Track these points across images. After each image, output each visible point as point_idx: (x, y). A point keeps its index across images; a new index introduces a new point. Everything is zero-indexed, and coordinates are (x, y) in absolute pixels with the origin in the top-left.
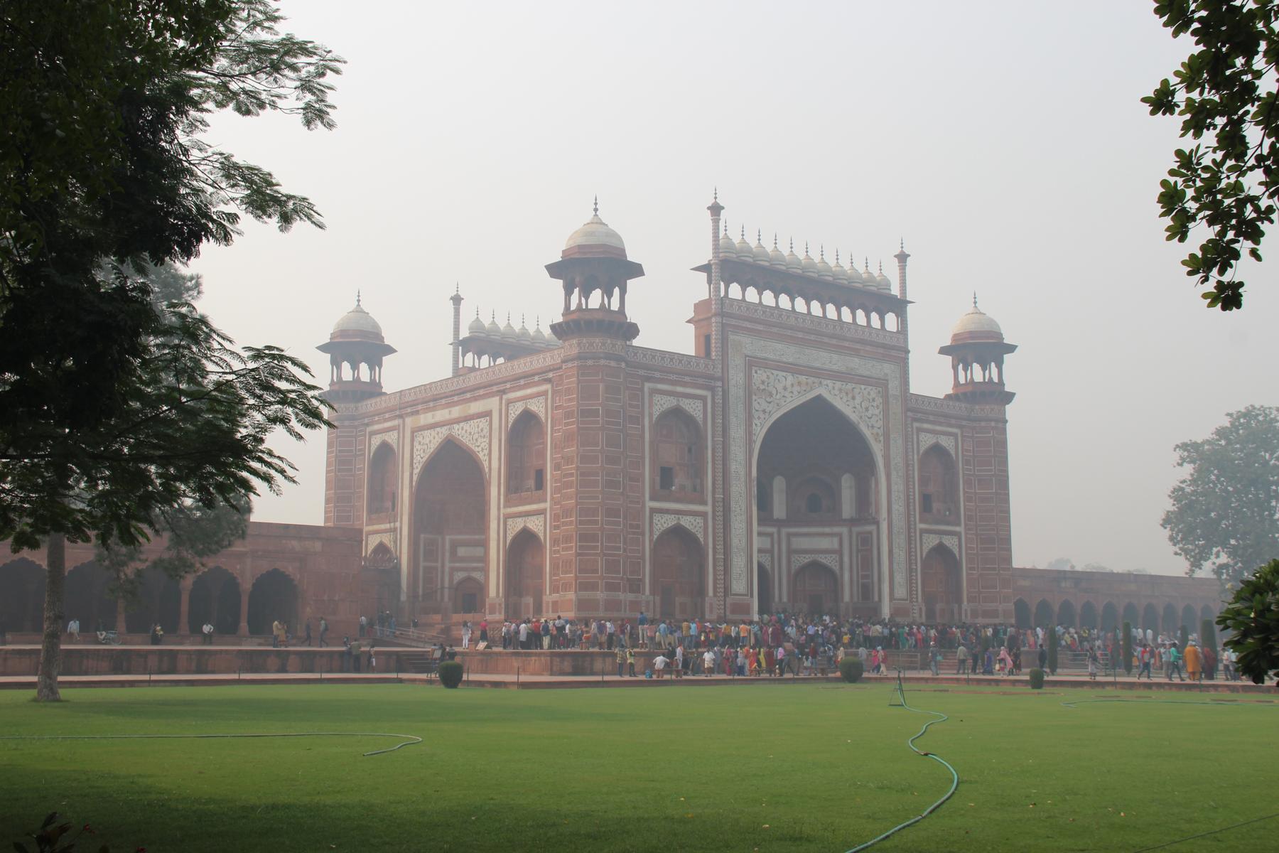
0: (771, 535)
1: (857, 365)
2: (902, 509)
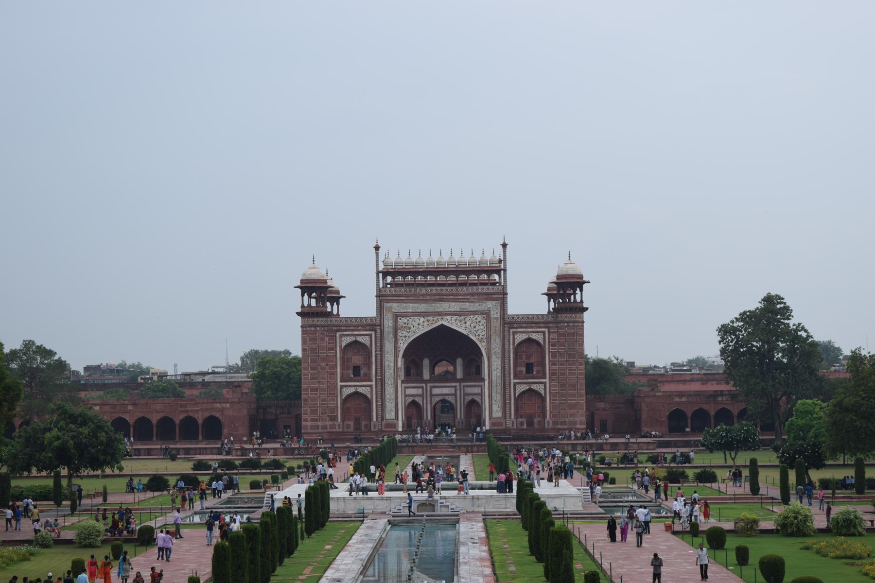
0: (455, 387)
1: (467, 306)
2: (499, 374)
